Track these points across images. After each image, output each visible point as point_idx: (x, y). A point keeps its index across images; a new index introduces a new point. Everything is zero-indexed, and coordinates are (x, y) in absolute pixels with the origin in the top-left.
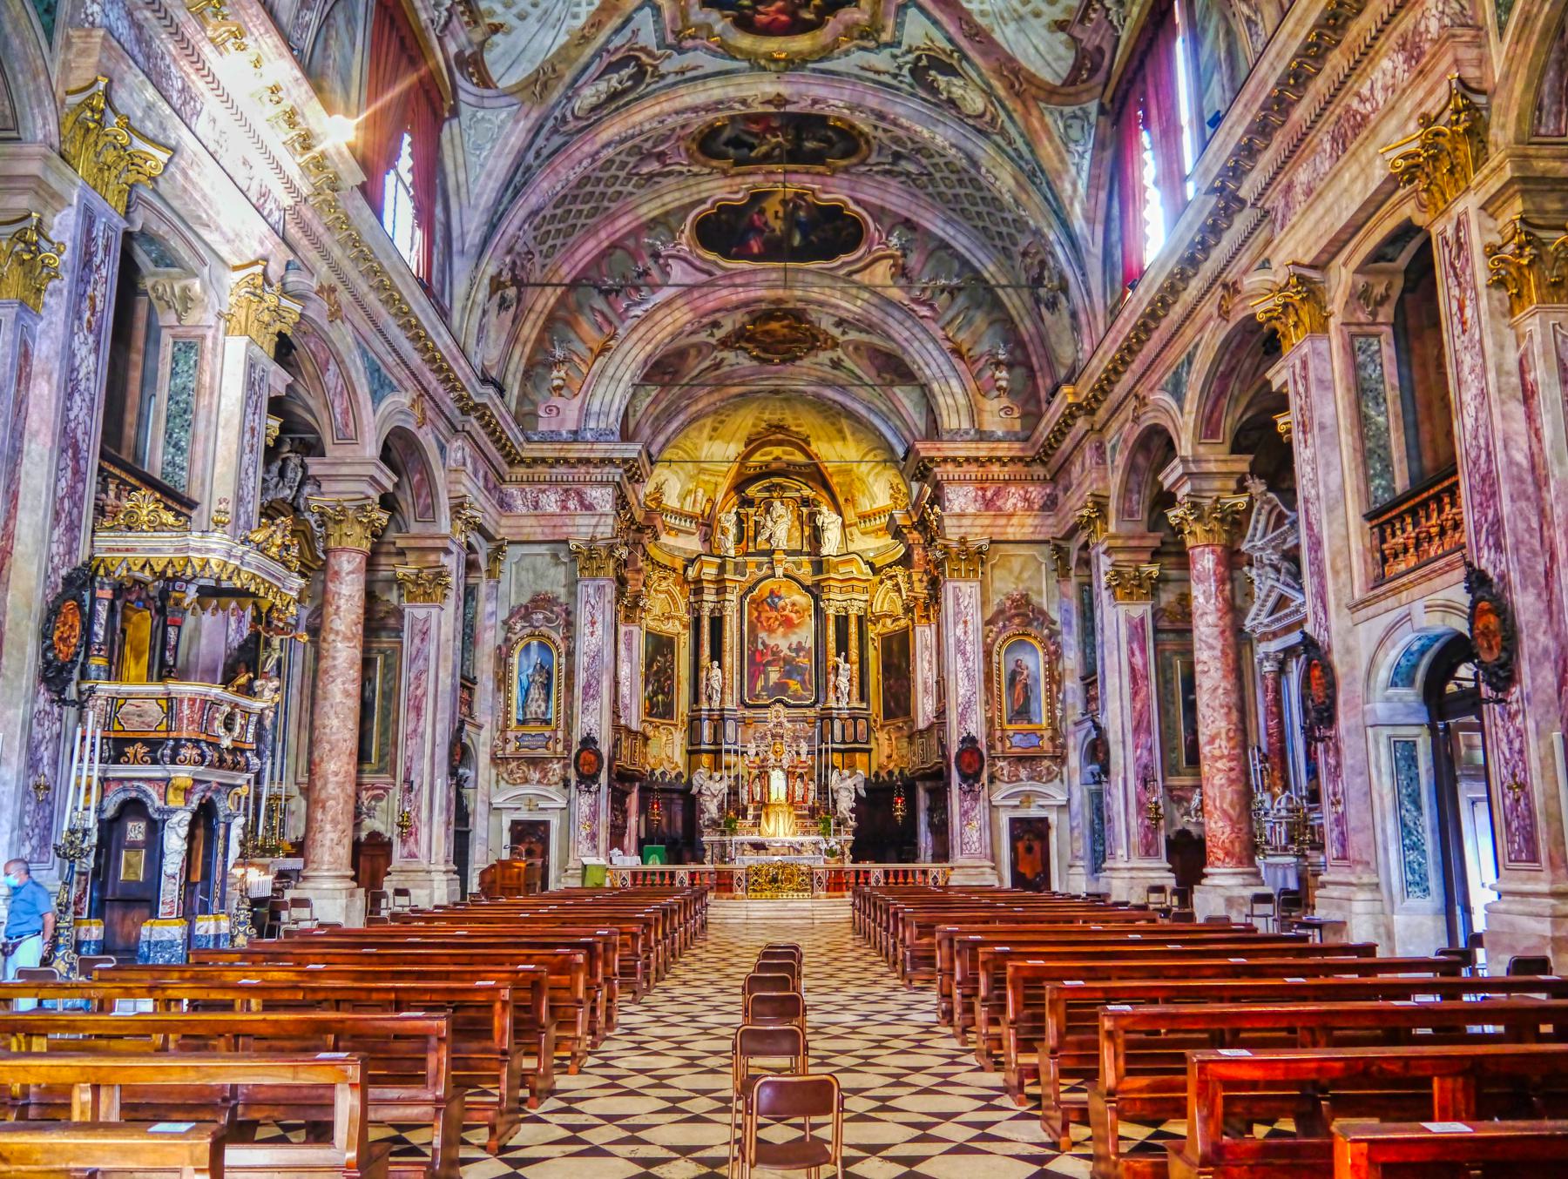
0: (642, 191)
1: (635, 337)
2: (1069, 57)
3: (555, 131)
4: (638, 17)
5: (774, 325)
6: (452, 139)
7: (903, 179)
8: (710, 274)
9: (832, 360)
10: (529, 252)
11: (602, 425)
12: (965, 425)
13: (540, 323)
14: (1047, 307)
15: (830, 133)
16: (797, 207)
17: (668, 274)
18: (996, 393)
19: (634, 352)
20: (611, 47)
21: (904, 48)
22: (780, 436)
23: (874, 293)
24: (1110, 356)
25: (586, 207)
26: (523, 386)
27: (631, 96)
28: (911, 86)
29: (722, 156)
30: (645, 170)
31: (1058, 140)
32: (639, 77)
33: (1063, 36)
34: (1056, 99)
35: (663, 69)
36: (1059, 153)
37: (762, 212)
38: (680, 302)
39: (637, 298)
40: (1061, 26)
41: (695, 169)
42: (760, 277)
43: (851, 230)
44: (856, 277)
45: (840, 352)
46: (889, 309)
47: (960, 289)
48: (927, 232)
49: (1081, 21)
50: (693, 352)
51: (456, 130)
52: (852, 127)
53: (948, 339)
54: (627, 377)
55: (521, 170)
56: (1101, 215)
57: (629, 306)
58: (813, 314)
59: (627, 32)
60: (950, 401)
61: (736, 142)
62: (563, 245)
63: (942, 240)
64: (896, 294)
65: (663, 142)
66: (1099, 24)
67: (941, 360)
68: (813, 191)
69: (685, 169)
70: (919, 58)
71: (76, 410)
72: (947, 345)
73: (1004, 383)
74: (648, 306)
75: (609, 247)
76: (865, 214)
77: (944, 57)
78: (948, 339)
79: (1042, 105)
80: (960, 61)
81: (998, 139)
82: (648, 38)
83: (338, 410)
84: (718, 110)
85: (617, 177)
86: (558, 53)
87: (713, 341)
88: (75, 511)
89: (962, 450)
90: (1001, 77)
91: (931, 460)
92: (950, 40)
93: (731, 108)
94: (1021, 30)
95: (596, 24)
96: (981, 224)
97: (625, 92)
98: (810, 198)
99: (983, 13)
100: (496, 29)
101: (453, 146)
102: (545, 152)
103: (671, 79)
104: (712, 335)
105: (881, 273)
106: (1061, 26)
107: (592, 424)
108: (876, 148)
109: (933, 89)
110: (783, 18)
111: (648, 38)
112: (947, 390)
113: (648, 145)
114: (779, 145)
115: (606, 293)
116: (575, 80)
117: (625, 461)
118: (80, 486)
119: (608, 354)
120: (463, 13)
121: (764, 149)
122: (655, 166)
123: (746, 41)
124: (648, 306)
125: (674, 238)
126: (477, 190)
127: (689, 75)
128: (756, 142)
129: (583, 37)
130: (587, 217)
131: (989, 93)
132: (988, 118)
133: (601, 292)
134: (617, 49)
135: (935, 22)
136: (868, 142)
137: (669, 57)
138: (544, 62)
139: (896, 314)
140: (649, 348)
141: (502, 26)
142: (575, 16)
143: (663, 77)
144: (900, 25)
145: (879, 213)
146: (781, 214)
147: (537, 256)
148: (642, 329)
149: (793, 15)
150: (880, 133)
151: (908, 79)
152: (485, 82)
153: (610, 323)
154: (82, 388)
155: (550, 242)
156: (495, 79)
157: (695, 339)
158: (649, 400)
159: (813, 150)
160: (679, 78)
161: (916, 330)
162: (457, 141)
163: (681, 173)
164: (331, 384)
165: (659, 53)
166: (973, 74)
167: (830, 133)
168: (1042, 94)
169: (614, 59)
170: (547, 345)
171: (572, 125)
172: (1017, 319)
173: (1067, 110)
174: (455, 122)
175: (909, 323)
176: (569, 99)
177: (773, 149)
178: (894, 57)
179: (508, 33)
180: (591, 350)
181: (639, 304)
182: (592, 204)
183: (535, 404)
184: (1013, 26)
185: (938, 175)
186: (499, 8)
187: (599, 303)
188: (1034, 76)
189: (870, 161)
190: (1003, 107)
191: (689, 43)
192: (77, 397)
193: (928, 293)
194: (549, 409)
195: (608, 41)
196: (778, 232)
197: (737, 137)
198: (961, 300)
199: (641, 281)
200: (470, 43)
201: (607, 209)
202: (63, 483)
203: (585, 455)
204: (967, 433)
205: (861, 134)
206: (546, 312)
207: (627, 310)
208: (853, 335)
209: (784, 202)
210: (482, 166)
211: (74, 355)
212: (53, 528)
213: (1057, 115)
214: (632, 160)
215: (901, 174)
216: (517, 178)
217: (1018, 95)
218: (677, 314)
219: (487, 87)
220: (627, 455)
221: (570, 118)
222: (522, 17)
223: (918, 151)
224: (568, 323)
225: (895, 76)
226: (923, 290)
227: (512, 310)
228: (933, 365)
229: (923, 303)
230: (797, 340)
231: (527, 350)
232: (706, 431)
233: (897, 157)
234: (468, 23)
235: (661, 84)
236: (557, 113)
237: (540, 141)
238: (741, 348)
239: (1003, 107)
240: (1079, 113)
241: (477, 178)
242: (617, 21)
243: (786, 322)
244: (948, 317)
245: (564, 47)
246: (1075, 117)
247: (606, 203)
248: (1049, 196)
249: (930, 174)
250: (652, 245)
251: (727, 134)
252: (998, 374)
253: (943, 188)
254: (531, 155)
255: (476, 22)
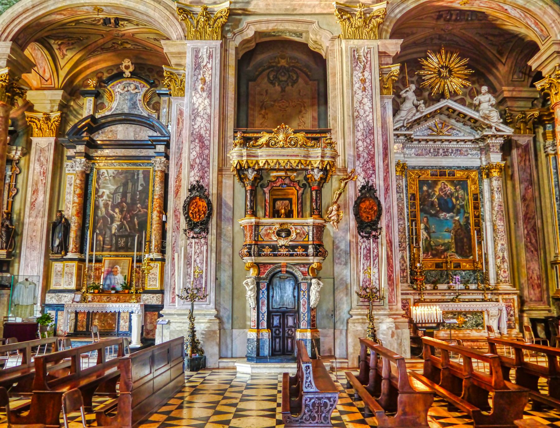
71: (198, 124)
83: (533, 26)
88: (205, 161)
118: (206, 152)
154: (201, 114)
164: (518, 16)
192: (199, 119)
202: (194, 153)
211: (194, 104)
212: (189, 172)
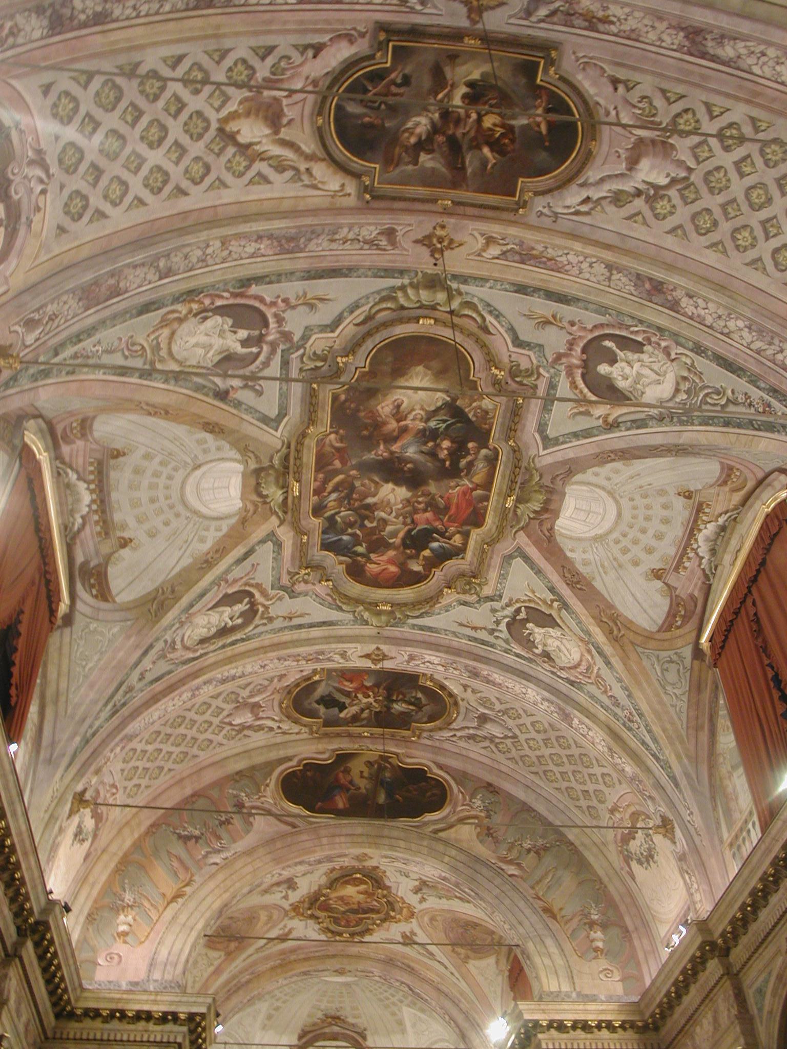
0: (232, 742)
1: (212, 885)
2: (664, 605)
3: (163, 656)
4: (260, 550)
5: (350, 891)
6: (60, 649)
7: (487, 743)
8: (294, 826)
9: (404, 936)
10: (114, 786)
11: (168, 977)
12: (565, 988)
13: (112, 865)
14: (640, 862)
15: (420, 695)
16: (381, 769)
17: (251, 824)
18: (594, 954)
19: (209, 900)
20: (230, 577)
21: (505, 600)
22: (336, 1029)
23: (461, 850)
24: (760, 873)
25: (177, 750)
26: (85, 929)
27: (238, 636)
28: (506, 641)
29: (312, 714)
30: (237, 721)
31: (657, 684)
32: (250, 614)
33: (659, 584)
34: (652, 644)
35: (272, 613)
36: (657, 695)
37: (347, 771)
38: (261, 851)
39: (217, 845)
40: (657, 574)
41: (285, 726)
42: (345, 831)
43: (435, 791)
44: (441, 834)
45: (414, 925)
46: (478, 867)
47: (546, 849)
48: (510, 796)
49: (676, 569)
50: (263, 916)
51: (66, 639)
52: (443, 687)
53: (539, 899)
54: (200, 926)
55: (124, 688)
56: (704, 754)
57: (208, 853)
58: (392, 878)
59: (247, 563)
60: (547, 961)
61: (328, 701)
62: (147, 787)
63: (524, 804)
64: (483, 850)
65: (260, 692)
66: (692, 572)
67: (534, 918)
68: (397, 754)
69: (275, 725)
70: (518, 611)
72: (538, 904)
73: (600, 944)
74: (228, 854)
75: (193, 796)
76: (448, 777)
77: (543, 609)
78: (539, 899)
79: (640, 650)
80: (560, 609)
81: (593, 689)
82: (265, 576)
84: (318, 660)
85: (211, 723)
86: (179, 574)
87: (286, 905)
89: (569, 1013)
90: (600, 622)
91: (536, 1024)
92: (552, 590)
93: (329, 660)
94: (620, 578)
95: (221, 550)
96: (564, 785)
97: (233, 629)
98: (395, 761)
99: (586, 563)
100: (124, 543)
101: (60, 654)
102: (149, 677)
103: (278, 624)
104: (286, 897)
105: (466, 833)
106: (657, 574)
107: (157, 975)
108: (463, 710)
109: (528, 643)
110: (393, 569)
111: (265, 576)
112: (544, 950)
113: (245, 693)
114: (369, 706)
115: (186, 839)
116: (191, 606)
117: (191, 1017)
119: (180, 900)
120: (97, 523)
121: (354, 710)
122: (245, 718)
123: (355, 589)
124: (228, 854)
125: (259, 791)
126: (76, 700)
127: (296, 621)
128: (347, 701)
129: (206, 561)
130: (175, 762)
131: (587, 641)
132: (582, 668)
133: (180, 837)
134: (235, 581)
135: (539, 572)
136: (456, 704)
137: (280, 599)
138: (164, 582)
139: (485, 871)
140: (226, 896)
141: (131, 540)
142: (202, 540)
143: (271, 619)
144: (503, 577)
145: (462, 778)
146: (366, 774)
147: (121, 791)
148: (221, 877)
149: (402, 566)
150: (469, 695)
151: (505, 634)
152: (104, 593)
153: (187, 869)
155: (135, 781)
156: (114, 592)
157: (269, 899)
158: (212, 969)
159: (402, 713)
160: (286, 623)
161: (506, 888)
162: (66, 649)
163: (271, 729)
165: (272, 593)
166: (572, 623)
167: (420, 695)
168: (638, 640)
169: (230, 591)
170: (118, 889)
171: (180, 654)
172: (605, 879)
173: (664, 654)
174: (67, 631)
175: (498, 881)
176: (182, 624)
177: (362, 710)
178: (494, 611)
179: (135, 549)
180: (164, 895)
181: (219, 851)
182: (182, 748)
183: (94, 950)
184: (612, 573)
185: (522, 737)
186: (132, 523)
187: (178, 848)
188: (631, 622)
189: (454, 726)
190: (601, 653)
191: (300, 587)
193: (514, 854)
194: (110, 957)
195: (228, 571)
196: (363, 791)
197: (329, 695)
198: (548, 860)
199: (222, 832)
200: (97, 553)
201: (196, 756)
203: (146, 1007)
204: (568, 995)
205: (451, 695)
206: (121, 854)
207: (205, 857)
208: (433, 903)
209: (369, 764)
210: (86, 677)
213: (654, 659)
214: (228, 707)
215: (485, 738)
216: (118, 697)
217: (616, 640)
218: (258, 864)
219: (106, 600)
220: (195, 1010)
221: (178, 646)
222: (152, 535)
223: (505, 712)
224: (142, 867)
225: (491, 632)
226: (510, 850)
227: (87, 844)
228: (526, 923)
229: (510, 862)
230: (372, 911)
231: (95, 893)
232: (261, 1017)
233: (483, 719)
234: (99, 534)
235: (269, 627)
236: (168, 637)
237: (147, 663)
238: (312, 916)
239: (601, 653)
240: (675, 658)
241: (79, 688)
242: (240, 551)
243: (363, 887)
244: (539, 873)
245: (185, 570)
246: (671, 661)
247: (195, 751)
248: (648, 739)
249: (515, 737)
250: (235, 796)
251: (321, 691)
252: (593, 935)
253: (527, 751)
254: (135, 675)
255: (107, 534)
